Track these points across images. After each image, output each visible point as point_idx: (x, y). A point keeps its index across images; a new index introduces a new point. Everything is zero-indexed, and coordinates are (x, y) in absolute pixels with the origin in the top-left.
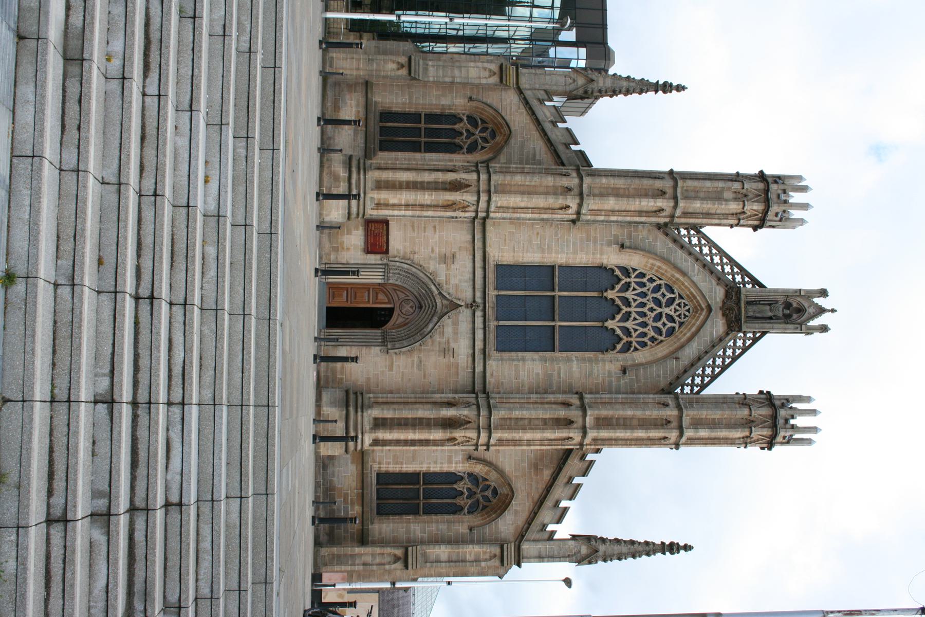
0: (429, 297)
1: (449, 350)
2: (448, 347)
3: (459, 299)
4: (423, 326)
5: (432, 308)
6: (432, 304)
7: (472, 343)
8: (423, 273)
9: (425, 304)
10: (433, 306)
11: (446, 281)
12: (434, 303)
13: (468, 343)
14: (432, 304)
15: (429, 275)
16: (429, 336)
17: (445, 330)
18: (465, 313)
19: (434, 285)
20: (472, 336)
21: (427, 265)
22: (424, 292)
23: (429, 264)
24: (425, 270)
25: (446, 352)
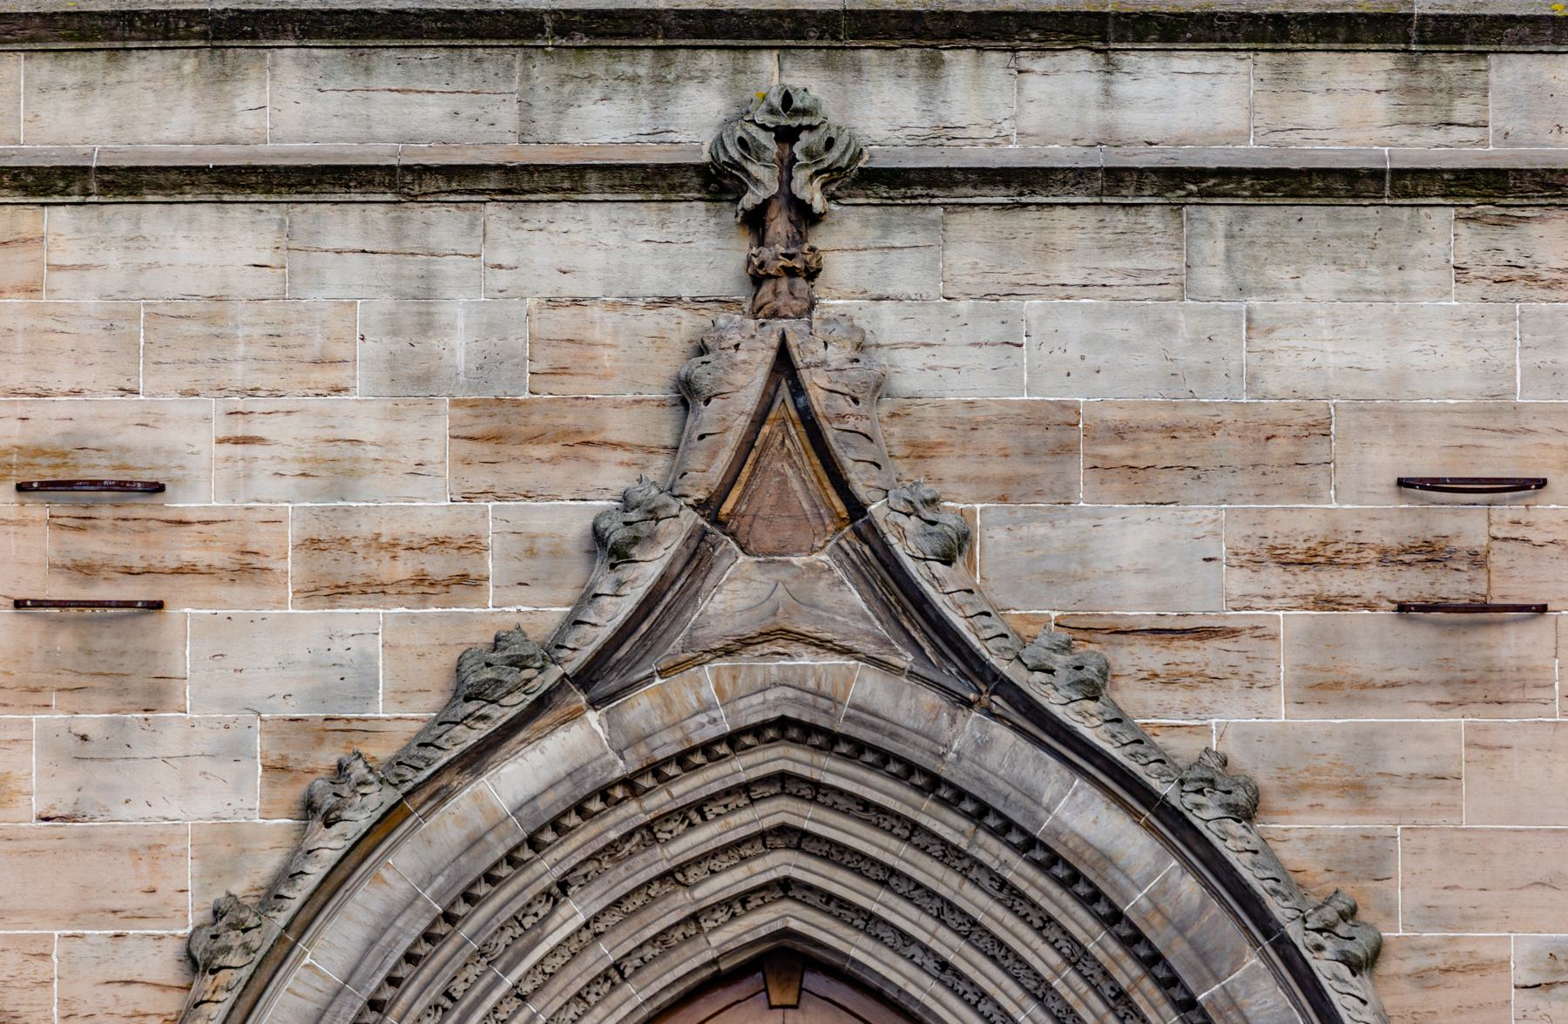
0: (649, 832)
1: (1431, 554)
2: (1386, 558)
3: (687, 395)
4: (1080, 922)
5: (816, 792)
6: (746, 791)
7: (1316, 218)
8: (301, 926)
9: (743, 900)
10: (783, 782)
11: (423, 585)
12: (740, 768)
13: (1322, 280)
14: (746, 791)
15: (330, 844)
16: (1232, 842)
17: (1139, 613)
18: (887, 323)
19: (475, 759)
20: (1218, 216)
21: (188, 872)
22: (573, 913)
23: (153, 849)
24: (272, 896)
25: (1454, 585)
